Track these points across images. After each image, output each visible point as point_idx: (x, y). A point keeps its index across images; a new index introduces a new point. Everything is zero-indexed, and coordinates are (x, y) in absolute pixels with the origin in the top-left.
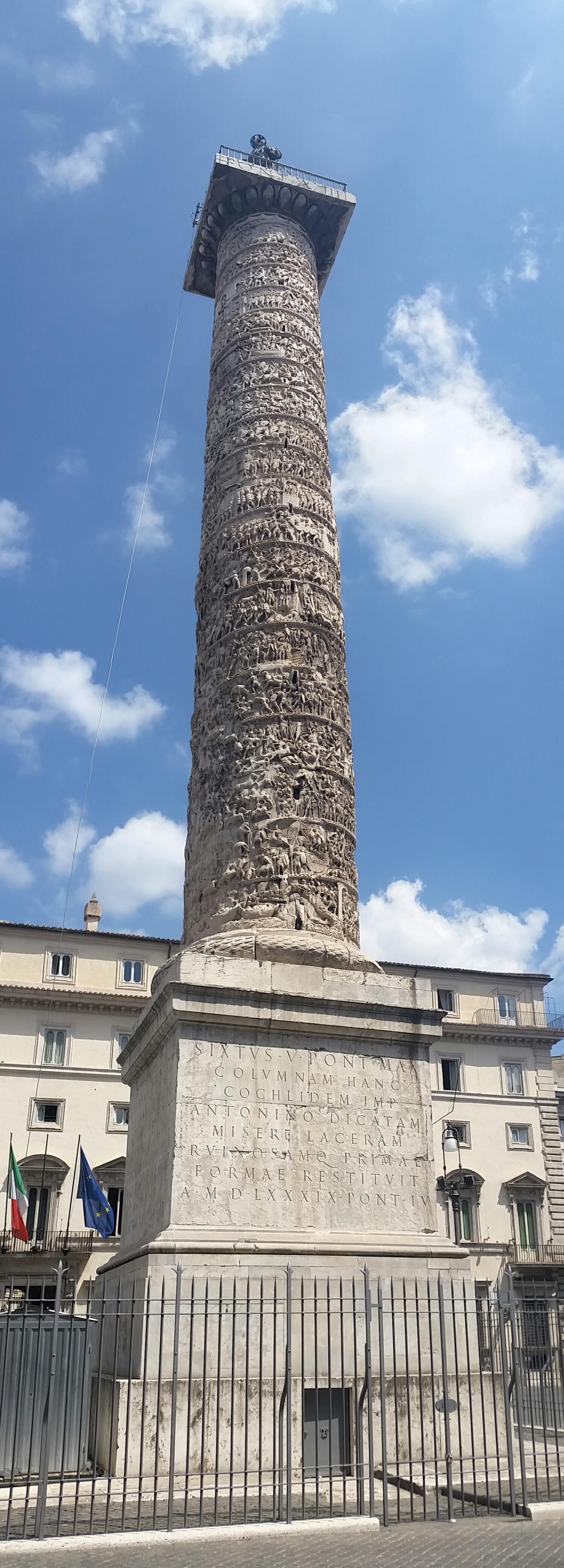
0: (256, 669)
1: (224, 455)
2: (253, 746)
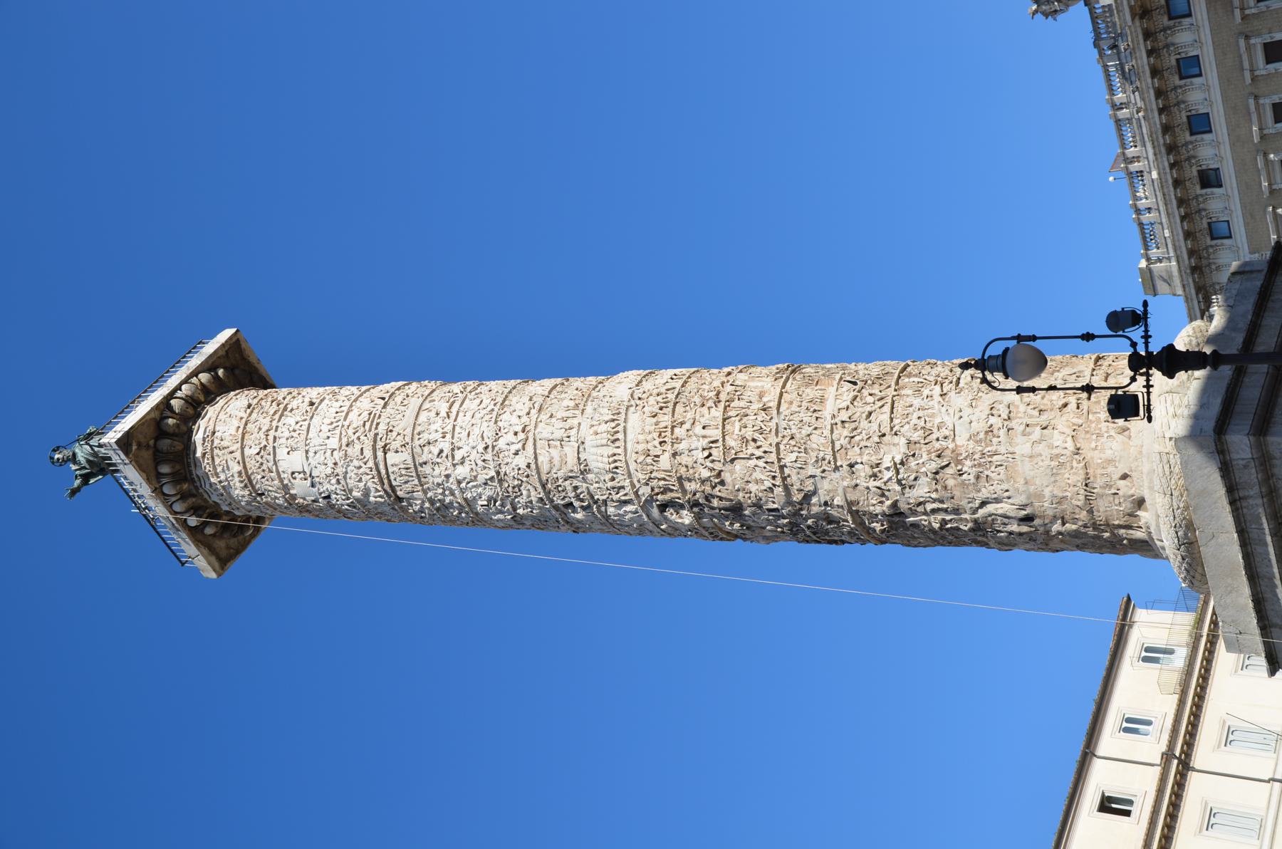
0: (829, 417)
1: (528, 466)
2: (923, 419)
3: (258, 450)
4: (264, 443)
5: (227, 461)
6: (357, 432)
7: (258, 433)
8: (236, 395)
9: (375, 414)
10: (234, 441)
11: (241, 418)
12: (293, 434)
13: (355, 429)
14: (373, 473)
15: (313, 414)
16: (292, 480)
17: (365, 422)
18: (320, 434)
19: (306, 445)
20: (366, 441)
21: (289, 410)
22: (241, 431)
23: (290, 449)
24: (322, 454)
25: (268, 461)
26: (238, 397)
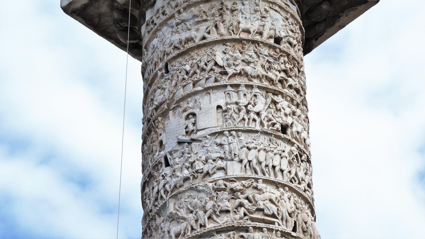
3: (220, 63)
5: (206, 20)
6: (250, 201)
7: (243, 61)
8: (292, 16)
9: (273, 223)
10: (231, 28)
11: (261, 34)
12: (244, 110)
13: (254, 197)
14: (199, 230)
15: (271, 134)
16: (185, 114)
17: (262, 210)
18: (245, 149)
19: (229, 131)
20: (237, 217)
21: (276, 98)
22: (244, 36)
23: (224, 108)
24: (219, 155)
25: (207, 79)
26: (291, 20)
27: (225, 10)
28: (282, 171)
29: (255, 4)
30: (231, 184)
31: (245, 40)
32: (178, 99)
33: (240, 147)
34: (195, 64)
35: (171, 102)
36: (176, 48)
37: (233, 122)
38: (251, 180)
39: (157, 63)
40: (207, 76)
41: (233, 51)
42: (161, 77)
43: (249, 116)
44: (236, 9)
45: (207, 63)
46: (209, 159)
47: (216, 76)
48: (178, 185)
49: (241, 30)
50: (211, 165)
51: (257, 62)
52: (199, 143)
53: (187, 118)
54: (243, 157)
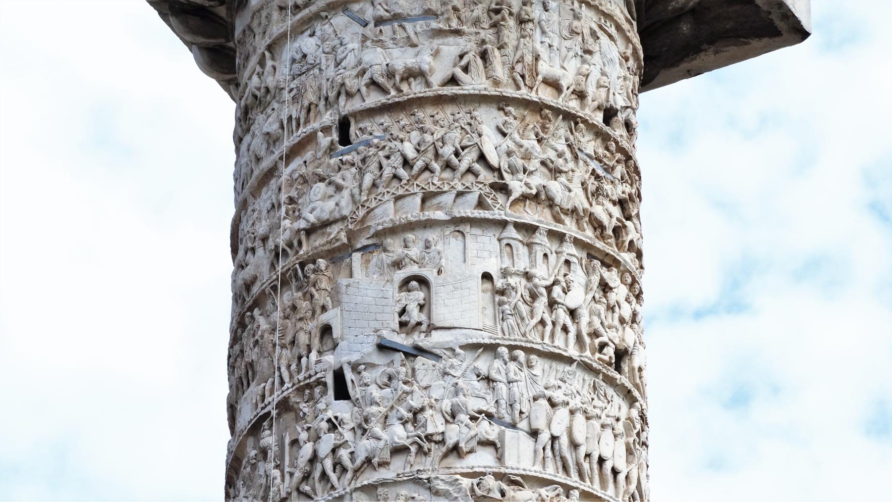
4: (517, 187)
5: (458, 33)
7: (543, 163)
12: (543, 300)
15: (596, 372)
18: (544, 402)
21: (606, 274)
25: (460, 194)
27: (507, 16)
28: (615, 472)
29: (572, 12)
30: (514, 490)
31: (550, 107)
32: (380, 228)
33: (531, 395)
34: (429, 146)
35: (360, 231)
36: (373, 84)
37: (518, 325)
38: (556, 489)
39: (312, 107)
40: (460, 188)
41: (521, 131)
42: (328, 151)
43: (554, 316)
44: (531, 18)
45: (461, 151)
46: (461, 411)
47: (482, 192)
48: (375, 461)
49: (540, 78)
50: (465, 430)
51: (573, 171)
52: (434, 362)
53: (405, 284)
54: (540, 423)
